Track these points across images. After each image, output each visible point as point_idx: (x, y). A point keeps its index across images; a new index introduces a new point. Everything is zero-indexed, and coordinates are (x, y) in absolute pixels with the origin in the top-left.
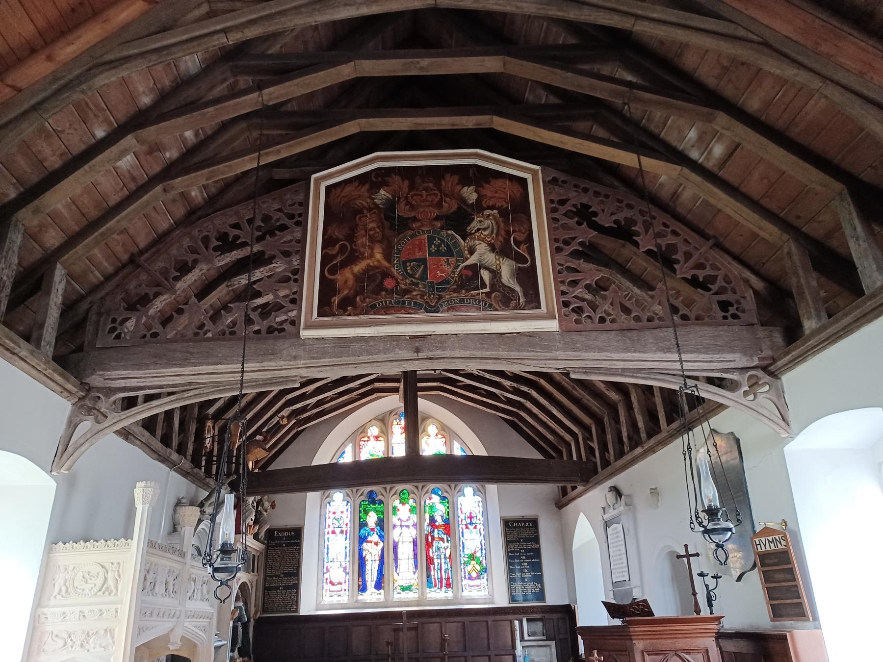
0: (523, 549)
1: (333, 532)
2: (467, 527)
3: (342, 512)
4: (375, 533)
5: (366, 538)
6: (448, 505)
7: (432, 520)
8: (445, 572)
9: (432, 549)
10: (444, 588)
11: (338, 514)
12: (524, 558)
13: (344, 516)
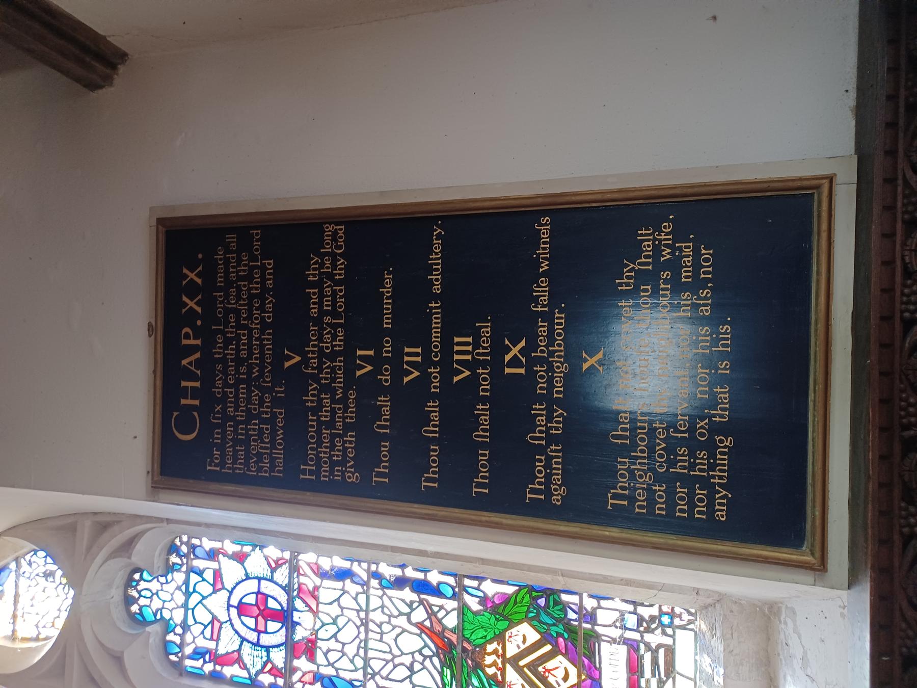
0: (349, 353)
2: (309, 648)
12: (412, 354)
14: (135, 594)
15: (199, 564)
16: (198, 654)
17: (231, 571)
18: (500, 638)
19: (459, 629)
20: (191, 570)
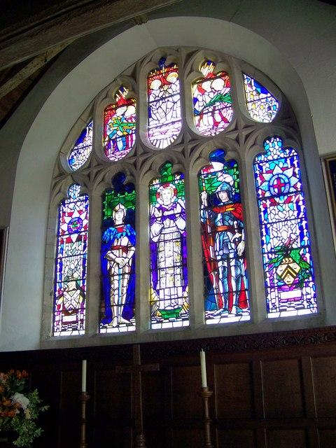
1: (69, 241)
2: (274, 204)
3: (80, 212)
4: (124, 234)
5: (111, 242)
6: (237, 172)
7: (214, 200)
8: (237, 281)
9: (213, 246)
10: (234, 310)
11: (76, 215)
13: (83, 217)
14: (272, 141)
15: (288, 161)
16: (261, 168)
17: (289, 173)
18: (294, 261)
19: (292, 249)
20: (286, 159)
